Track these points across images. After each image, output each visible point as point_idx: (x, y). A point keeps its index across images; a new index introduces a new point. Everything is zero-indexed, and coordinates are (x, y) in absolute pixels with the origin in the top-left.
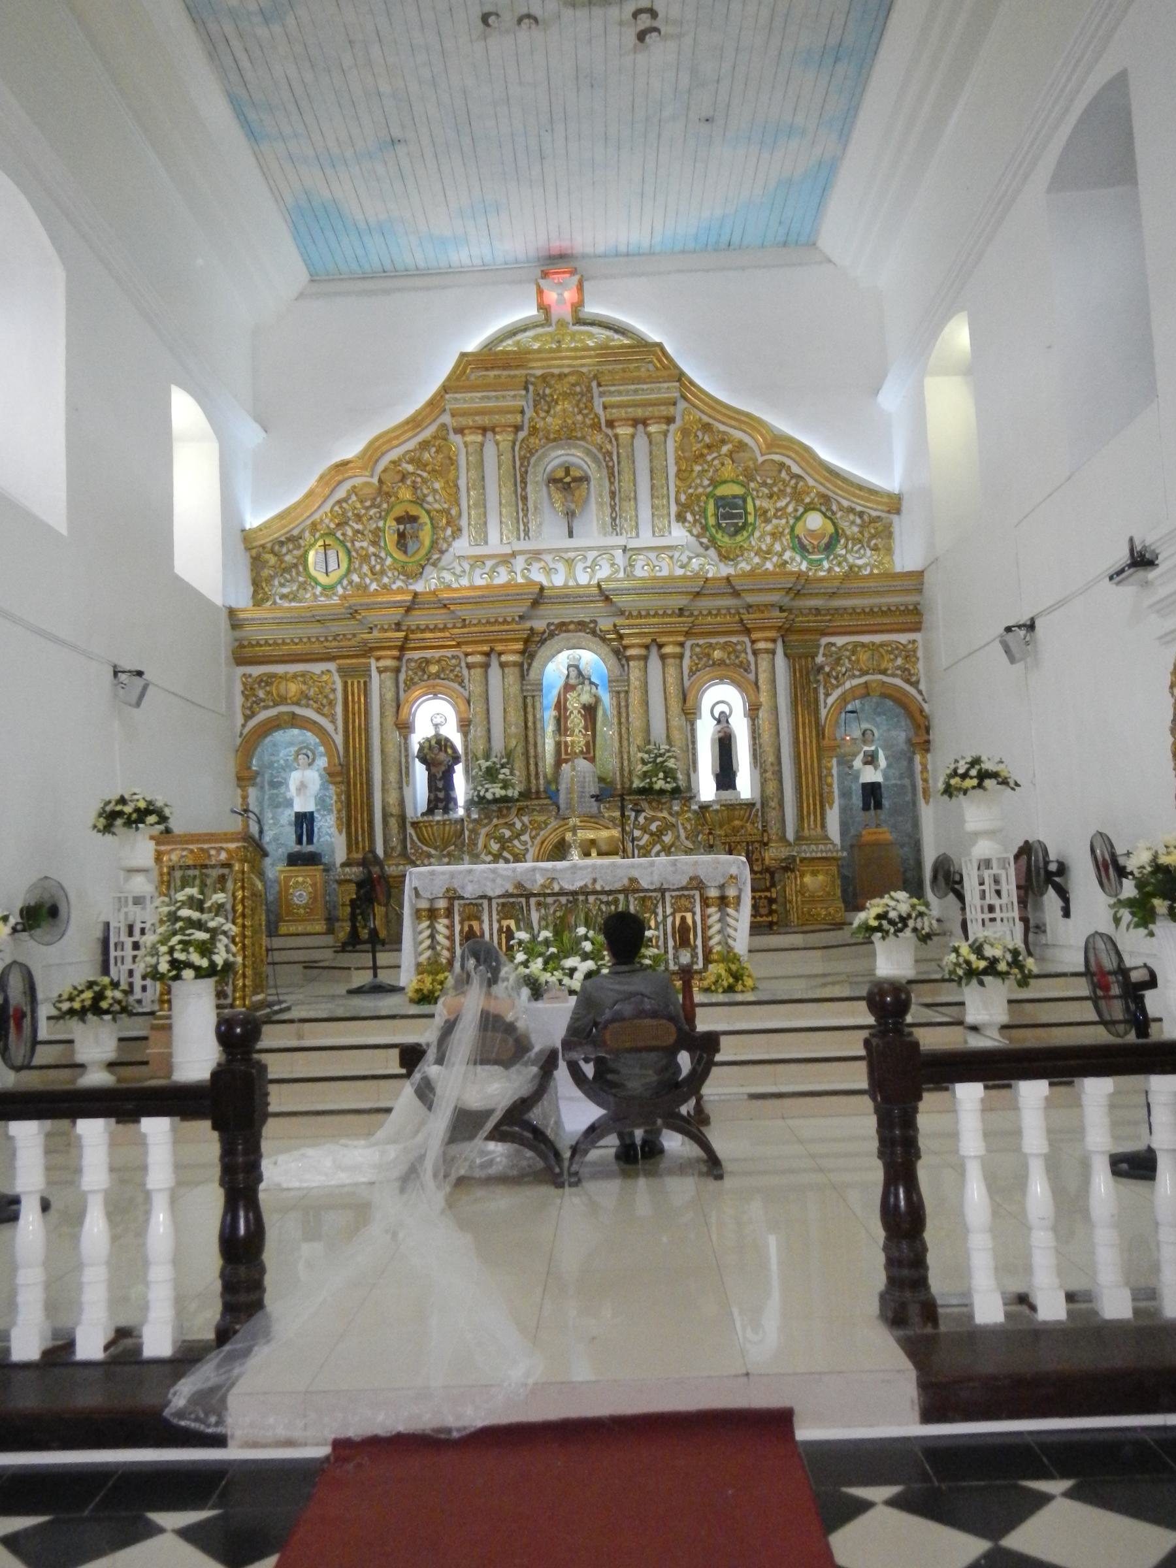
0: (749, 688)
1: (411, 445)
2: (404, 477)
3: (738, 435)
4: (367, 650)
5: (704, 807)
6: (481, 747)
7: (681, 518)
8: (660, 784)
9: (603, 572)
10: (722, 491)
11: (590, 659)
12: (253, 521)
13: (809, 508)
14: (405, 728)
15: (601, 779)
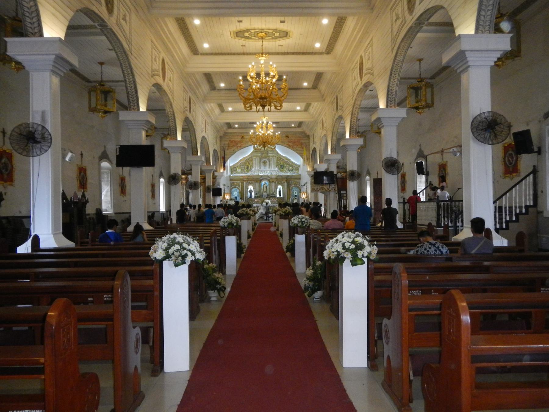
0: (283, 186)
1: (248, 158)
2: (247, 161)
3: (283, 158)
4: (244, 181)
5: (278, 198)
6: (255, 191)
7: (277, 167)
8: (273, 195)
9: (268, 173)
10: (281, 164)
11: (267, 182)
12: (231, 165)
13: (290, 166)
14: (248, 189)
15: (267, 194)
